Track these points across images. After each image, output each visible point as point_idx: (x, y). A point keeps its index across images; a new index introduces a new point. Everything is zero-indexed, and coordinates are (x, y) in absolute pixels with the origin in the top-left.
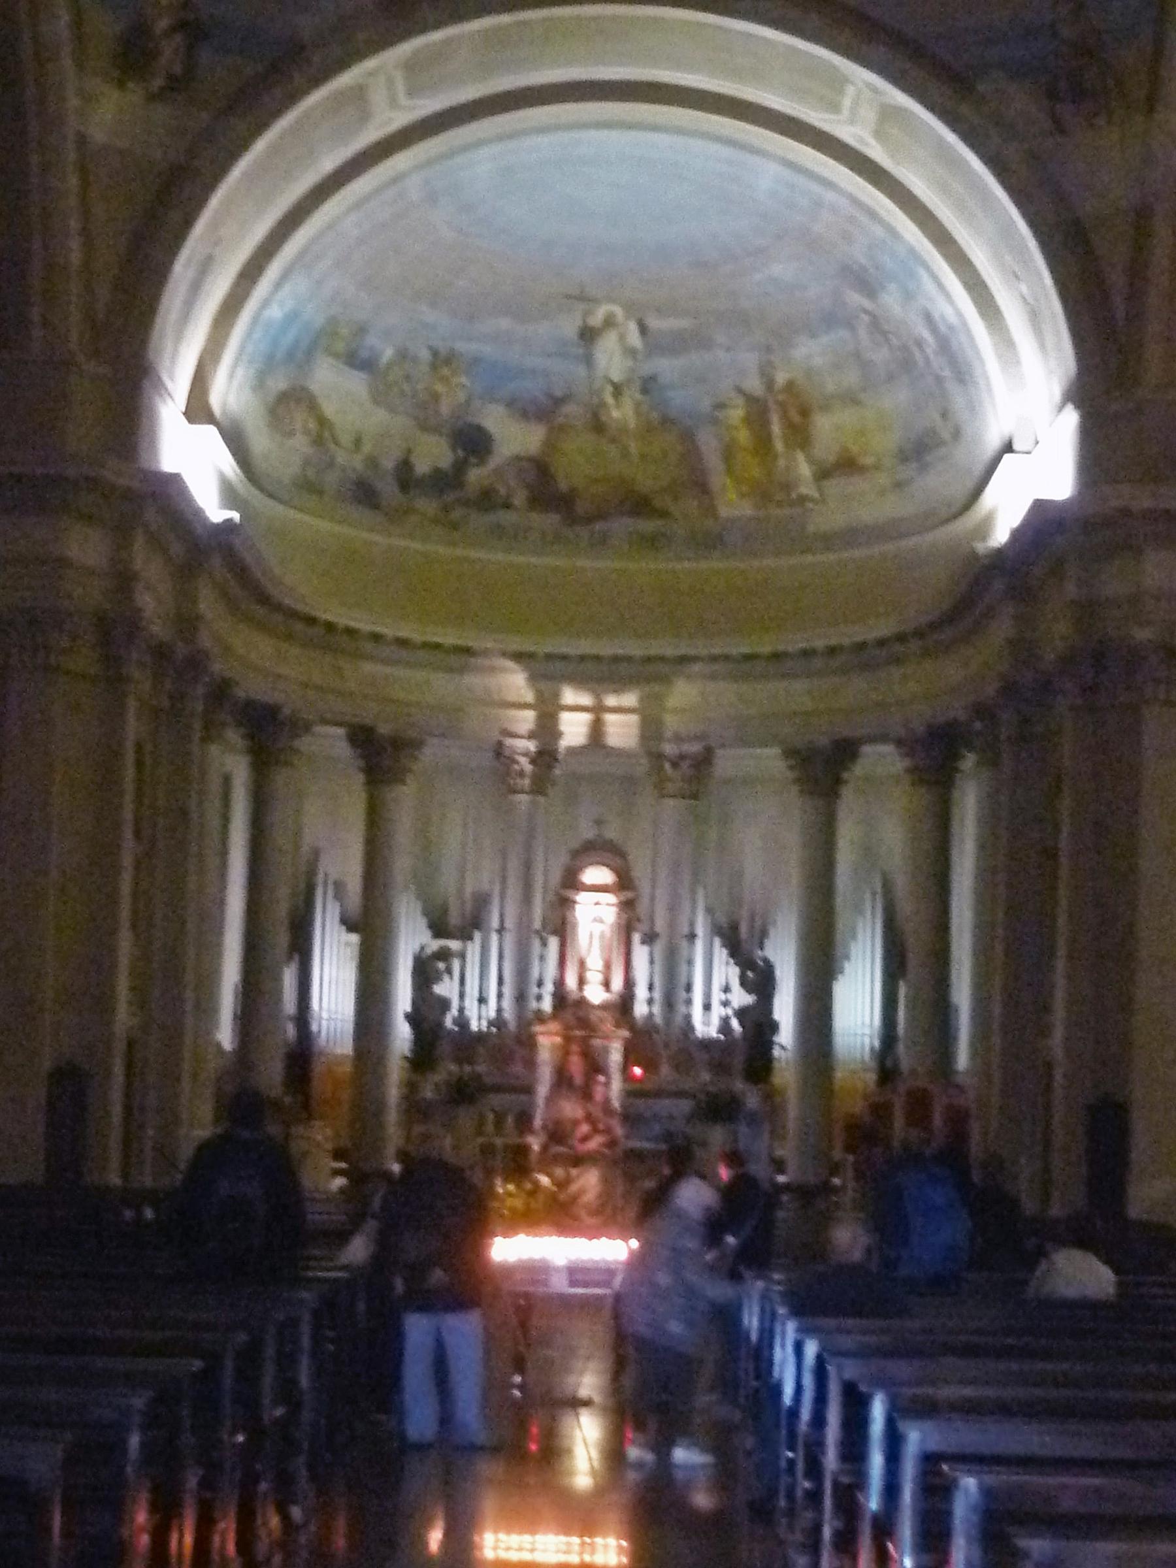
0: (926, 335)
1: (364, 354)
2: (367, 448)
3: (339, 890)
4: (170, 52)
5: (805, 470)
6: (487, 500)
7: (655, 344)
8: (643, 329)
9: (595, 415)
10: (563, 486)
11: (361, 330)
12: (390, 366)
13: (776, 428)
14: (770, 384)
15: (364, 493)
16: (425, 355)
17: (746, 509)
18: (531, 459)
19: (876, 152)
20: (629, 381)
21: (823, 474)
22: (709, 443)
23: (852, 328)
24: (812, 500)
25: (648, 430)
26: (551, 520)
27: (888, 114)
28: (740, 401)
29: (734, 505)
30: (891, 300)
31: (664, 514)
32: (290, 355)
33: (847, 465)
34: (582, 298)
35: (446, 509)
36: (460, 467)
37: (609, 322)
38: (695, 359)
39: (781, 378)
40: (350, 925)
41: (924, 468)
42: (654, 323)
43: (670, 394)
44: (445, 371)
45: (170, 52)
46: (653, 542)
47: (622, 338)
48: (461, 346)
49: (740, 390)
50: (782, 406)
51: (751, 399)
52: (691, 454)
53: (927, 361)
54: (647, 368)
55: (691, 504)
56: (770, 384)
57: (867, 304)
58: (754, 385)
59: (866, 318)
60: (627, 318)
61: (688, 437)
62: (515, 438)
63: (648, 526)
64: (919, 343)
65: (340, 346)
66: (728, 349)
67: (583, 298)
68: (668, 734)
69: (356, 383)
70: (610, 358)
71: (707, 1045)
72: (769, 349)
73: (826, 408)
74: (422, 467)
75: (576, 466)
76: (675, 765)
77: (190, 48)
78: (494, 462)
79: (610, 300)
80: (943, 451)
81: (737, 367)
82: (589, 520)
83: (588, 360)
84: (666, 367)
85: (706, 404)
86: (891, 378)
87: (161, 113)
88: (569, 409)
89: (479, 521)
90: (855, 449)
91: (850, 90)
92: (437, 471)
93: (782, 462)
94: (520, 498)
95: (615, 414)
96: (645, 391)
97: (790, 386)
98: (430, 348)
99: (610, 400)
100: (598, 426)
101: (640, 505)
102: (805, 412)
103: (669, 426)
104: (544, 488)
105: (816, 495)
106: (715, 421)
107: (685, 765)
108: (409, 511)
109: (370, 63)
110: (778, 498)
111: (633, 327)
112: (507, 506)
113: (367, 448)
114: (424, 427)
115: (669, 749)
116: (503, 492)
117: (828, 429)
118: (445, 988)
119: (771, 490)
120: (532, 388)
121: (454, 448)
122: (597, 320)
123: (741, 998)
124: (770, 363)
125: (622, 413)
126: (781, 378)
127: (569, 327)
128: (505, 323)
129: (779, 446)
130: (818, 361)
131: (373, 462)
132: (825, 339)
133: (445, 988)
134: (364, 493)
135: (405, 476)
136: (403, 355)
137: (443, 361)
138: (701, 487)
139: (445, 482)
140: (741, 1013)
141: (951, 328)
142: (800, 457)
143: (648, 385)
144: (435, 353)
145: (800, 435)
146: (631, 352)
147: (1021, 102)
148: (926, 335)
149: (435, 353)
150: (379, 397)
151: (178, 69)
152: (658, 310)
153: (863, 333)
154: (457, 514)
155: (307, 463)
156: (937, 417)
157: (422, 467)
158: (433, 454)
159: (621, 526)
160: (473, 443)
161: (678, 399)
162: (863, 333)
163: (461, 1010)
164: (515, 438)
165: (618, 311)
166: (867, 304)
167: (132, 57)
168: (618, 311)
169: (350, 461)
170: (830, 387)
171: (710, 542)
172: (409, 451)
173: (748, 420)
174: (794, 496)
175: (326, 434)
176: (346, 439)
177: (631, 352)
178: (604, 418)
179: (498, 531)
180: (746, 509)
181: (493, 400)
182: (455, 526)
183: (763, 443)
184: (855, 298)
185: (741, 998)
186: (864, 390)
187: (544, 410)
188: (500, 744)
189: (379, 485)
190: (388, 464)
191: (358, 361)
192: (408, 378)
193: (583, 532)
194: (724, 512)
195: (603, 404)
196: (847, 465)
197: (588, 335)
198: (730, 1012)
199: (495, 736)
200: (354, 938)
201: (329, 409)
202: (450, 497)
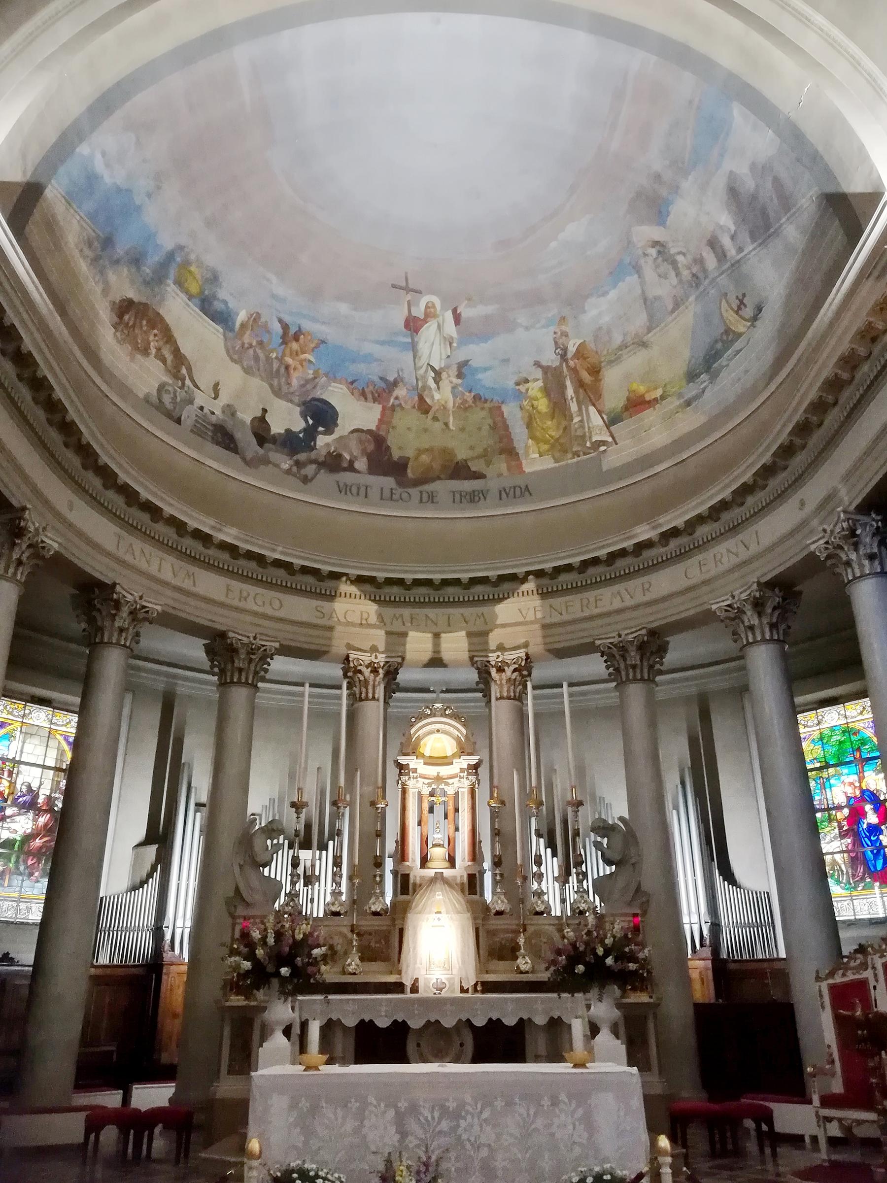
1: (218, 306)
2: (224, 399)
5: (596, 420)
6: (334, 463)
8: (457, 319)
9: (421, 398)
10: (396, 454)
11: (214, 279)
12: (243, 326)
13: (570, 392)
14: (564, 357)
15: (223, 437)
16: (277, 328)
17: (548, 463)
18: (369, 432)
20: (448, 367)
21: (612, 421)
22: (512, 413)
23: (637, 269)
24: (604, 443)
25: (463, 408)
26: (389, 482)
28: (539, 374)
29: (535, 461)
32: (136, 260)
33: (637, 404)
34: (407, 289)
35: (297, 463)
36: (311, 433)
37: (429, 314)
38: (501, 343)
39: (572, 349)
41: (714, 377)
42: (466, 312)
43: (480, 376)
44: (295, 346)
46: (473, 498)
47: (439, 326)
48: (307, 325)
49: (537, 364)
50: (574, 371)
51: (546, 370)
52: (500, 428)
53: (722, 256)
54: (461, 358)
55: (501, 465)
57: (656, 233)
58: (550, 358)
59: (653, 252)
60: (444, 309)
61: (496, 411)
62: (356, 415)
63: (468, 485)
65: (194, 289)
66: (527, 328)
68: (493, 645)
69: (212, 332)
70: (433, 346)
72: (563, 319)
73: (615, 360)
74: (277, 428)
75: (409, 439)
76: (500, 670)
78: (339, 432)
79: (433, 293)
80: (737, 345)
82: (417, 483)
84: (477, 353)
85: (511, 384)
86: (677, 305)
88: (400, 392)
89: (324, 477)
90: (642, 389)
93: (576, 420)
94: (361, 464)
95: (437, 396)
96: (460, 375)
97: (580, 353)
98: (280, 321)
99: (431, 383)
100: (424, 407)
101: (459, 471)
102: (595, 371)
103: (481, 403)
105: (610, 439)
106: (519, 396)
107: (509, 671)
108: (266, 461)
110: (575, 449)
111: (449, 315)
112: (351, 468)
113: (224, 399)
114: (277, 393)
115: (492, 657)
116: (347, 457)
119: (567, 442)
120: (371, 372)
121: (304, 416)
122: (419, 311)
124: (565, 334)
125: (442, 395)
126: (572, 349)
127: (398, 317)
128: (344, 308)
129: (574, 407)
130: (606, 319)
131: (230, 410)
132: (613, 294)
134: (223, 437)
135: (261, 430)
136: (255, 319)
137: (291, 335)
138: (510, 452)
140: (600, 885)
142: (592, 409)
143: (462, 369)
144: (285, 327)
145: (590, 392)
149: (285, 327)
150: (236, 355)
152: (469, 299)
153: (649, 273)
154: (310, 470)
155: (162, 388)
156: (730, 316)
157: (277, 428)
158: (286, 418)
159: (443, 487)
160: (321, 415)
161: (487, 379)
162: (649, 273)
163: (293, 896)
164: (356, 415)
166: (656, 233)
170: (618, 339)
172: (265, 411)
173: (546, 391)
174: (588, 444)
175: (184, 371)
176: (205, 380)
178: (428, 400)
179: (344, 490)
180: (548, 463)
181: (335, 380)
182: (306, 480)
183: (559, 407)
186: (649, 330)
187: (380, 392)
188: (347, 658)
189: (238, 435)
190: (247, 416)
192: (261, 343)
193: (414, 492)
194: (528, 469)
195: (425, 387)
196: (637, 404)
197: (413, 325)
198: (588, 884)
199: (343, 651)
201: (186, 348)
202: (302, 457)
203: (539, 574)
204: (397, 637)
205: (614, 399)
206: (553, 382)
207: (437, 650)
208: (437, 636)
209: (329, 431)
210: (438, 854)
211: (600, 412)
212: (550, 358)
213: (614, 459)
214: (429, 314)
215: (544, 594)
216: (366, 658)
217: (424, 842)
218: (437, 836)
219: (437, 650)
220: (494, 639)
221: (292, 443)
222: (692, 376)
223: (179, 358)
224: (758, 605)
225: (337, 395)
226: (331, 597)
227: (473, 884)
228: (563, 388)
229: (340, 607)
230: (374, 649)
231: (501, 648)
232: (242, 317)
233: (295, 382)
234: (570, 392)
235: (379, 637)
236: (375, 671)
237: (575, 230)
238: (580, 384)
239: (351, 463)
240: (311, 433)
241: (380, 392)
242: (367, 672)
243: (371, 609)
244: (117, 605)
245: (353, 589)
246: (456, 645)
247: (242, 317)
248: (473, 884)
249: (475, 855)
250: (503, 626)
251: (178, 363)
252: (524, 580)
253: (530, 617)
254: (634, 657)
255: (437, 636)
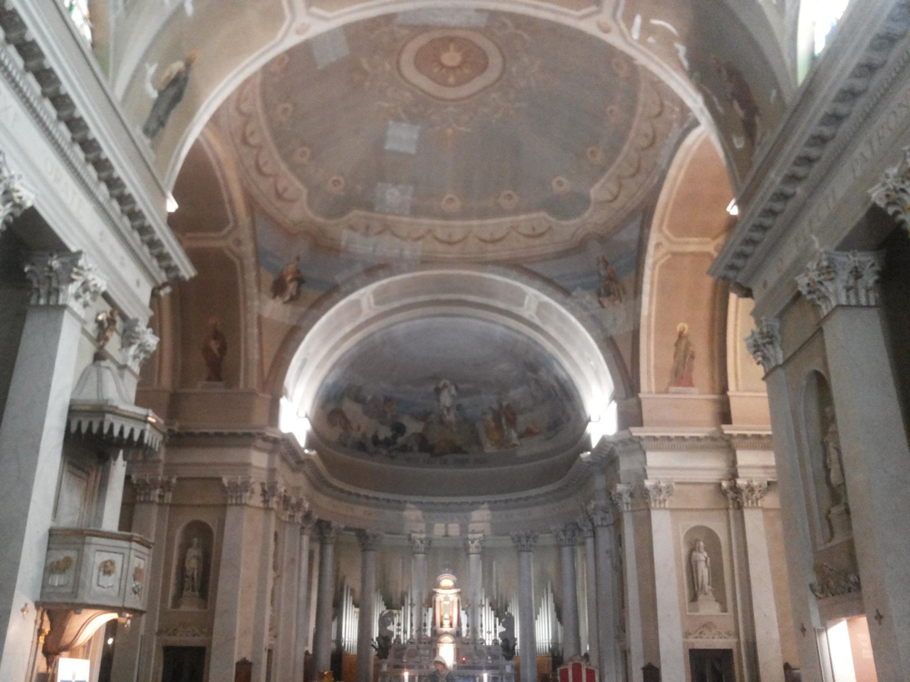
0: (555, 384)
3: (353, 591)
4: (292, 287)
5: (514, 435)
6: (404, 449)
7: (461, 393)
8: (457, 389)
13: (504, 421)
15: (361, 446)
19: (537, 321)
21: (521, 436)
22: (480, 426)
26: (427, 455)
27: (542, 305)
29: (490, 449)
30: (542, 373)
31: (465, 453)
33: (529, 433)
36: (395, 437)
37: (445, 386)
40: (357, 606)
42: (460, 386)
45: (292, 287)
46: (462, 463)
47: (449, 392)
49: (491, 409)
53: (556, 395)
56: (501, 405)
58: (495, 406)
62: (413, 427)
63: (459, 456)
64: (553, 387)
67: (435, 378)
70: (446, 399)
71: (489, 648)
74: (381, 437)
77: (299, 286)
81: (489, 400)
83: (438, 400)
84: (465, 401)
87: (289, 308)
88: (433, 417)
91: (527, 298)
92: (386, 438)
94: (416, 448)
95: (448, 418)
97: (508, 406)
99: (445, 412)
100: (441, 422)
101: (457, 450)
102: (514, 414)
104: (425, 445)
109: (362, 291)
112: (411, 450)
114: (382, 423)
115: (470, 536)
116: (409, 445)
117: (522, 421)
118: (392, 628)
119: (503, 442)
123: (501, 629)
125: (451, 417)
126: (505, 403)
127: (431, 388)
129: (505, 427)
131: (364, 435)
133: (392, 628)
134: (361, 446)
135: (376, 441)
137: (388, 400)
138: (478, 443)
139: (388, 443)
140: (501, 634)
141: (566, 381)
143: (459, 407)
145: (512, 422)
146: (453, 396)
147: (588, 298)
148: (555, 384)
151: (294, 293)
157: (381, 437)
158: (385, 433)
160: (399, 429)
164: (413, 427)
165: (448, 382)
167: (278, 288)
168: (448, 382)
169: (356, 435)
171: (482, 461)
177: (453, 396)
182: (392, 458)
183: (499, 427)
184: (529, 374)
185: (501, 629)
187: (424, 417)
190: (370, 436)
191: (358, 399)
197: (438, 391)
200: (358, 610)
201: (349, 417)
202: (391, 447)
203: (489, 502)
204: (430, 528)
205: (522, 427)
206: (497, 417)
207: (447, 532)
208: (446, 526)
209: (402, 435)
210: (446, 623)
211: (516, 431)
212: (495, 406)
213: (522, 452)
214: (445, 386)
215: (490, 509)
216: (418, 536)
217: (442, 617)
218: (446, 616)
219: (447, 532)
220: (471, 527)
221: (388, 443)
222: (549, 429)
223: (347, 422)
224: (564, 532)
225: (406, 420)
226: (403, 509)
227: (458, 634)
228: (501, 420)
229: (407, 513)
230: (421, 532)
231: (473, 532)
232: (369, 398)
233: (389, 416)
234: (504, 421)
235: (422, 526)
236: (422, 542)
237: (504, 366)
238: (508, 420)
239: (411, 447)
240: (395, 437)
241: (424, 417)
242: (418, 542)
243: (419, 514)
244: (331, 529)
245: (413, 506)
246: (454, 529)
247: (369, 398)
248: (458, 634)
249: (459, 624)
250: (475, 522)
251: (346, 423)
252: (483, 503)
253: (486, 519)
254: (524, 541)
255: (446, 526)
